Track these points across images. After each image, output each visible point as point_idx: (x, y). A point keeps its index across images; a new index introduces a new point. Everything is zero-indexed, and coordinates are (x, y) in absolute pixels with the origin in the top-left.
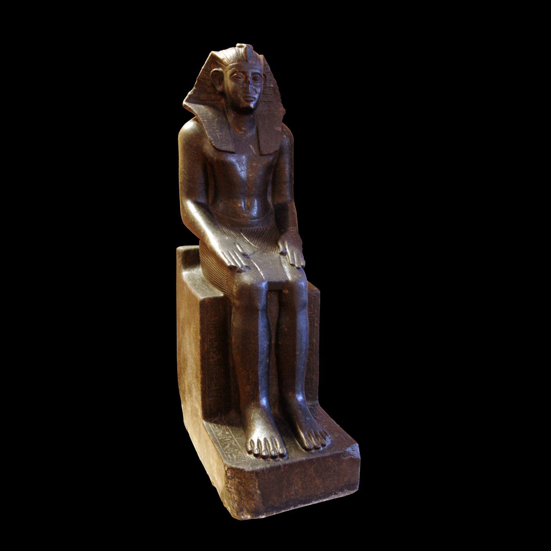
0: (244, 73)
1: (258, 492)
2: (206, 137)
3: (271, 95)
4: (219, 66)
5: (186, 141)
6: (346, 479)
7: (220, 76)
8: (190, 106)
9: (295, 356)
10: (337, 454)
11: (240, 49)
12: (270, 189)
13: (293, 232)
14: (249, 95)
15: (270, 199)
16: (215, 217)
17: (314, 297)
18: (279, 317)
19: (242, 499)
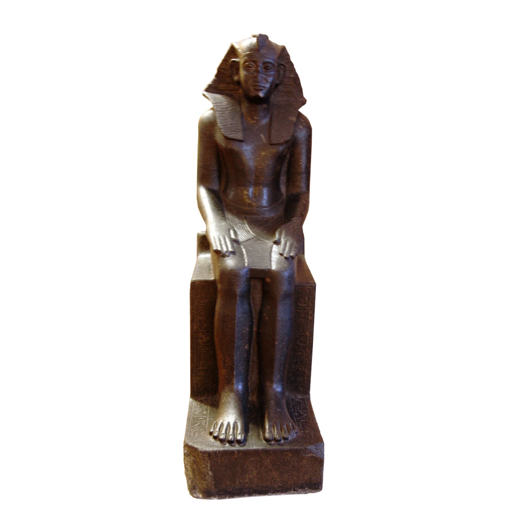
0: (255, 62)
1: (210, 473)
6: (306, 477)
9: (274, 345)
10: (297, 449)
12: (283, 179)
13: (296, 222)
15: (283, 189)
16: (224, 203)
17: (309, 289)
18: (262, 305)
19: (195, 477)
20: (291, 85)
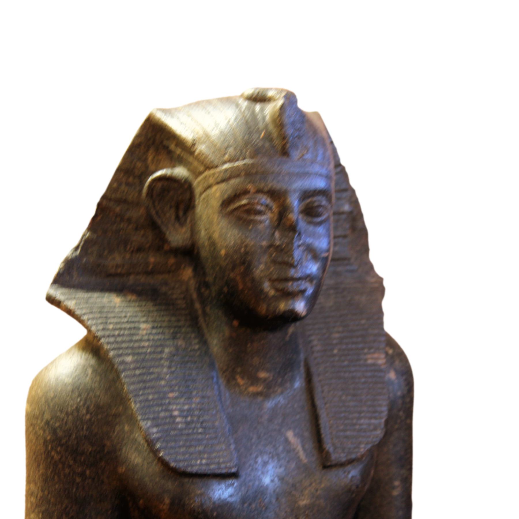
2: (132, 420)
3: (345, 237)
4: (175, 160)
5: (54, 431)
7: (179, 197)
8: (71, 304)
11: (258, 107)
14: (292, 272)
20: (345, 237)
